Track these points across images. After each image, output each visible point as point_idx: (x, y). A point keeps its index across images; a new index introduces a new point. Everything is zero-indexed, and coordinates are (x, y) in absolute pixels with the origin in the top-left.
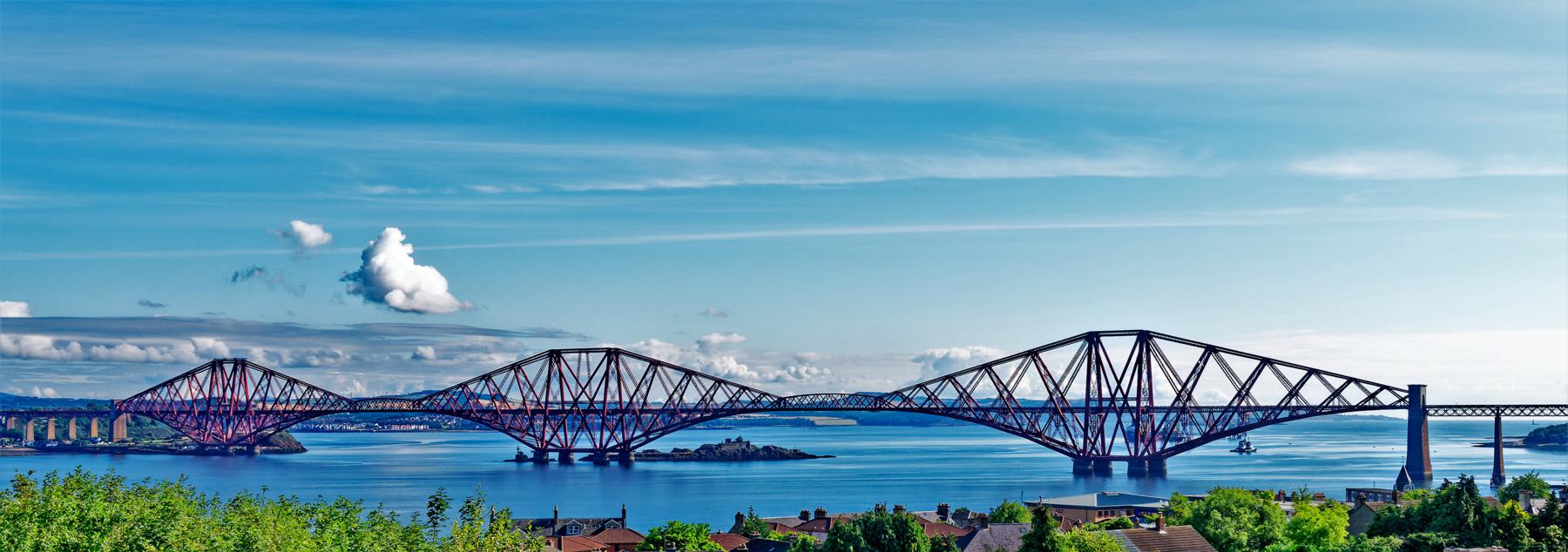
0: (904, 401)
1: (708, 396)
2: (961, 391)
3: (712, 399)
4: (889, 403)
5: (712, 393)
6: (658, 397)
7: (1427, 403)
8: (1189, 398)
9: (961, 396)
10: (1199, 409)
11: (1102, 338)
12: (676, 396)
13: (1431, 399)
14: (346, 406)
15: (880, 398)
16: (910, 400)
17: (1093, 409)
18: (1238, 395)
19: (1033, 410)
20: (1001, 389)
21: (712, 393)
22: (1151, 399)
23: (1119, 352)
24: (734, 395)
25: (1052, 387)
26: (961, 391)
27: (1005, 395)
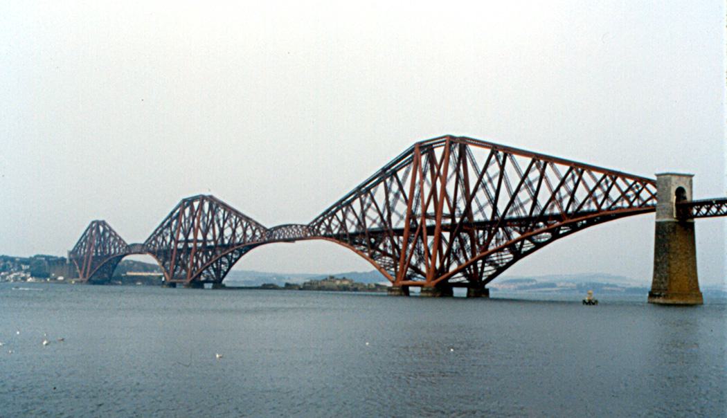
1: (563, 191)
3: (572, 200)
12: (524, 196)
21: (571, 185)
24: (598, 185)
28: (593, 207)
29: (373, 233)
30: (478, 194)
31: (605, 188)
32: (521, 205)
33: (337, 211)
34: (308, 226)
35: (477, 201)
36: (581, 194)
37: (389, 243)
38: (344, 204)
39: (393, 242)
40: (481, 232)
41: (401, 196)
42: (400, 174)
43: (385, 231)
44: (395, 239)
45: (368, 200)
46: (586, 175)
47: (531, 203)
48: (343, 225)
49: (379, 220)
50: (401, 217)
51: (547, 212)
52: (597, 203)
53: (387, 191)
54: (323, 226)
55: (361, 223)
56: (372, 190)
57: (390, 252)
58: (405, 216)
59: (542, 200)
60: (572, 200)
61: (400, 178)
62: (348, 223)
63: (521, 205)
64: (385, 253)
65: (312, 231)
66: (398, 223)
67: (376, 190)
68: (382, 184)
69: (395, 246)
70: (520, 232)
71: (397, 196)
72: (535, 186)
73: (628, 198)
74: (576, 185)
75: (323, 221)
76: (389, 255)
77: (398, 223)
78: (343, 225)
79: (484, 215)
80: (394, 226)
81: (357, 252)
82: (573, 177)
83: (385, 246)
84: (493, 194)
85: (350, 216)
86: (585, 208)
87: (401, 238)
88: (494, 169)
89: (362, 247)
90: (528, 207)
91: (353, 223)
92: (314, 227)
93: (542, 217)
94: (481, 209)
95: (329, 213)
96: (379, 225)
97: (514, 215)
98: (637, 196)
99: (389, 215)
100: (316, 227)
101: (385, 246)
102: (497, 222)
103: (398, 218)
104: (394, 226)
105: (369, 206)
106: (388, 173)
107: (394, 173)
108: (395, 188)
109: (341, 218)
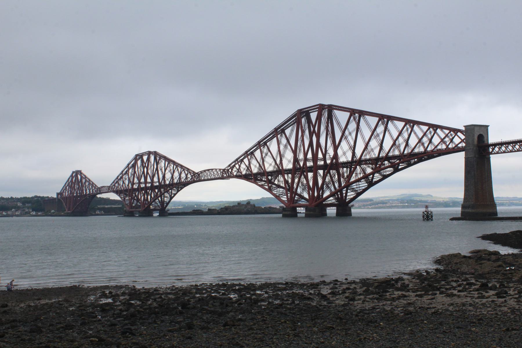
1: (401, 140)
5: (405, 135)
21: (405, 135)
28: (422, 149)
29: (271, 173)
30: (342, 144)
31: (430, 136)
32: (372, 150)
34: (224, 170)
35: (342, 148)
36: (413, 141)
38: (249, 154)
40: (345, 169)
41: (289, 147)
42: (288, 132)
43: (280, 171)
45: (265, 150)
46: (416, 128)
47: (379, 148)
48: (249, 168)
49: (273, 164)
50: (290, 161)
51: (391, 154)
52: (424, 147)
54: (235, 169)
55: (261, 166)
56: (268, 144)
58: (292, 161)
60: (407, 145)
61: (288, 136)
62: (252, 167)
63: (372, 150)
64: (279, 186)
69: (286, 182)
70: (372, 169)
71: (285, 146)
72: (381, 136)
73: (445, 143)
74: (409, 135)
75: (234, 166)
76: (282, 187)
77: (288, 165)
78: (249, 168)
79: (346, 157)
81: (260, 186)
82: (407, 130)
85: (254, 162)
86: (416, 150)
87: (290, 175)
88: (353, 126)
89: (263, 183)
91: (255, 166)
92: (228, 170)
93: (387, 158)
94: (344, 153)
95: (239, 161)
96: (274, 167)
97: (368, 157)
98: (452, 141)
100: (230, 170)
101: (279, 181)
105: (266, 155)
107: (283, 131)
108: (284, 141)
109: (247, 163)
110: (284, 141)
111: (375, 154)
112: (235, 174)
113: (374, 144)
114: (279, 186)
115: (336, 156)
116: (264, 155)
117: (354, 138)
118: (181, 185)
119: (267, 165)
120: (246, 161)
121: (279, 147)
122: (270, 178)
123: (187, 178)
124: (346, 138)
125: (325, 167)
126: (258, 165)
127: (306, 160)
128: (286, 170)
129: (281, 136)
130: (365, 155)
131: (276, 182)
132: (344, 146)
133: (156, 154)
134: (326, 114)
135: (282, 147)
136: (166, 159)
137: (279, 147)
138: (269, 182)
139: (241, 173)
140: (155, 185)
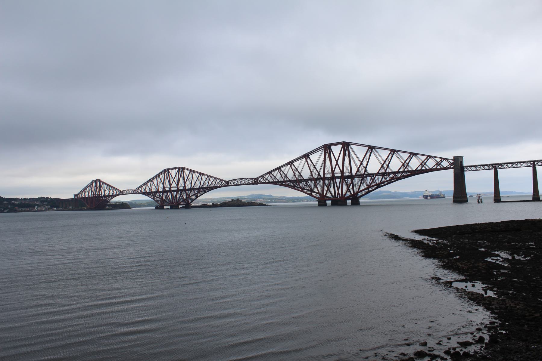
0: (263, 179)
2: (281, 173)
4: (260, 181)
6: (374, 167)
7: (464, 165)
8: (366, 171)
9: (281, 176)
10: (370, 175)
11: (332, 147)
13: (466, 163)
14: (224, 184)
15: (257, 179)
16: (267, 179)
17: (328, 178)
18: (403, 165)
19: (307, 180)
20: (295, 172)
22: (351, 172)
23: (358, 152)
25: (312, 168)
26: (281, 173)
27: (297, 173)
29: (154, 192)
30: (187, 182)
33: (143, 186)
34: (134, 190)
35: (187, 184)
37: (158, 195)
38: (145, 184)
39: (159, 194)
40: (188, 191)
41: (161, 182)
42: (161, 176)
43: (158, 192)
44: (160, 194)
45: (152, 183)
47: (199, 184)
48: (145, 190)
49: (155, 189)
50: (161, 188)
53: (157, 181)
54: (139, 190)
55: (150, 189)
56: (153, 181)
57: (159, 197)
58: (162, 188)
59: (202, 183)
61: (161, 178)
62: (147, 190)
63: (197, 185)
64: (157, 197)
65: (135, 192)
66: (161, 189)
67: (154, 180)
68: (156, 179)
70: (197, 192)
71: (160, 182)
72: (200, 180)
75: (139, 189)
77: (161, 189)
78: (145, 190)
79: (188, 187)
80: (159, 190)
81: (150, 197)
83: (157, 195)
84: (191, 182)
85: (147, 187)
87: (162, 193)
88: (190, 176)
89: (151, 196)
90: (214, 185)
91: (148, 189)
92: (136, 190)
93: (202, 188)
94: (188, 186)
95: (141, 187)
96: (155, 190)
99: (158, 188)
100: (137, 190)
101: (157, 195)
102: (192, 189)
103: (160, 188)
104: (159, 190)
105: (152, 185)
106: (157, 176)
107: (159, 176)
108: (159, 180)
109: (144, 188)
110: (159, 180)
111: (198, 186)
112: (139, 192)
113: (198, 183)
114: (157, 197)
115: (105, 194)
116: (151, 185)
117: (191, 180)
118: (114, 196)
119: (152, 189)
120: (144, 187)
121: (157, 183)
122: (154, 194)
123: (116, 193)
124: (189, 180)
125: (181, 191)
126: (149, 189)
127: (91, 195)
128: (160, 191)
129: (158, 178)
130: (204, 186)
131: (156, 196)
132: (188, 183)
133: (100, 181)
134: (181, 170)
135: (158, 183)
136: (106, 184)
137: (157, 183)
138: (154, 196)
139: (142, 192)
140: (336, 175)
